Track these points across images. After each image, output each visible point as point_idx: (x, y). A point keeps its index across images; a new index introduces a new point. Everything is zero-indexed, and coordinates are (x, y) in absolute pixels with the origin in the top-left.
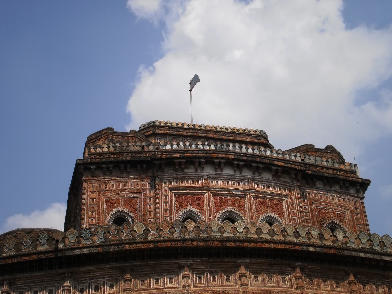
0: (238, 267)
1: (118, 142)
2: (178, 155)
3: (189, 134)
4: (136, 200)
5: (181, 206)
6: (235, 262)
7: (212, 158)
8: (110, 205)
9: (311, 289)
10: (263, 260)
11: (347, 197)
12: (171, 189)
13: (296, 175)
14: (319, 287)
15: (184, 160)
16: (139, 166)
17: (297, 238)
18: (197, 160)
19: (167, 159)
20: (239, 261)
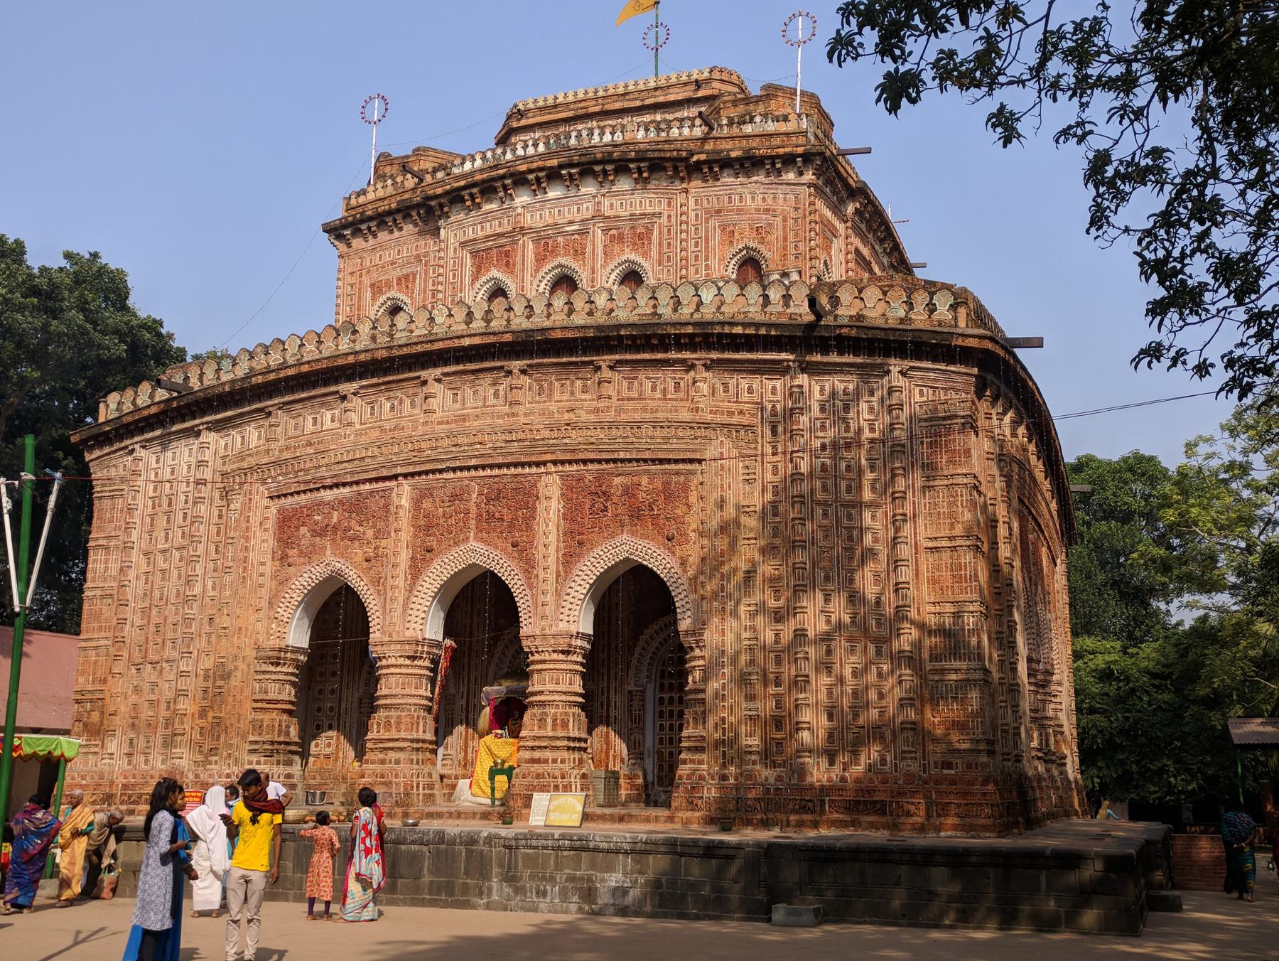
0: (425, 383)
1: (392, 177)
2: (462, 183)
3: (570, 114)
4: (414, 276)
5: (478, 272)
6: (419, 377)
7: (523, 173)
8: (377, 289)
9: (538, 402)
10: (461, 367)
11: (781, 190)
12: (463, 244)
13: (675, 169)
14: (550, 396)
15: (475, 190)
16: (414, 213)
17: (528, 317)
18: (498, 184)
19: (447, 193)
20: (424, 374)
